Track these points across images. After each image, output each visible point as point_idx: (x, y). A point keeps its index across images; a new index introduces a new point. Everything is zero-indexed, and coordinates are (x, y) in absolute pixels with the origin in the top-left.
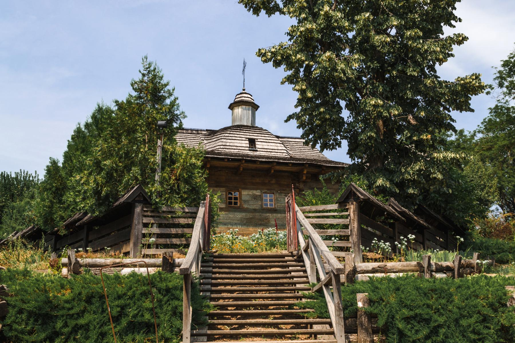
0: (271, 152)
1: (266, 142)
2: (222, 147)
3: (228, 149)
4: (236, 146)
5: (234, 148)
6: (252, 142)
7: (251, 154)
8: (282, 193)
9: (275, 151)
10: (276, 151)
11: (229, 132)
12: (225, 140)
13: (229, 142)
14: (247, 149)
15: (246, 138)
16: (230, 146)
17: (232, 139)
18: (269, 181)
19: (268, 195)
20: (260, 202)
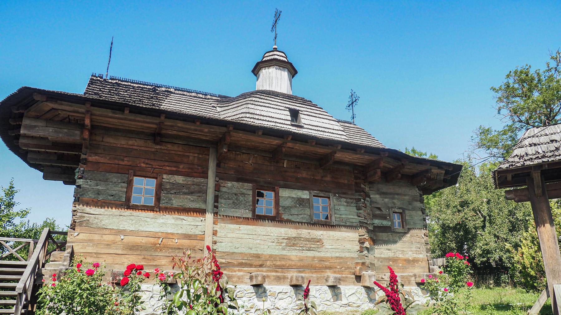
0: (324, 132)
1: (315, 117)
2: (248, 115)
3: (258, 119)
4: (271, 117)
5: (268, 119)
6: (295, 114)
7: (295, 131)
8: (342, 197)
9: (330, 131)
10: (332, 131)
11: (258, 96)
12: (253, 106)
13: (258, 110)
14: (289, 123)
15: (286, 107)
16: (261, 115)
17: (264, 106)
18: (322, 177)
19: (320, 199)
20: (308, 210)
